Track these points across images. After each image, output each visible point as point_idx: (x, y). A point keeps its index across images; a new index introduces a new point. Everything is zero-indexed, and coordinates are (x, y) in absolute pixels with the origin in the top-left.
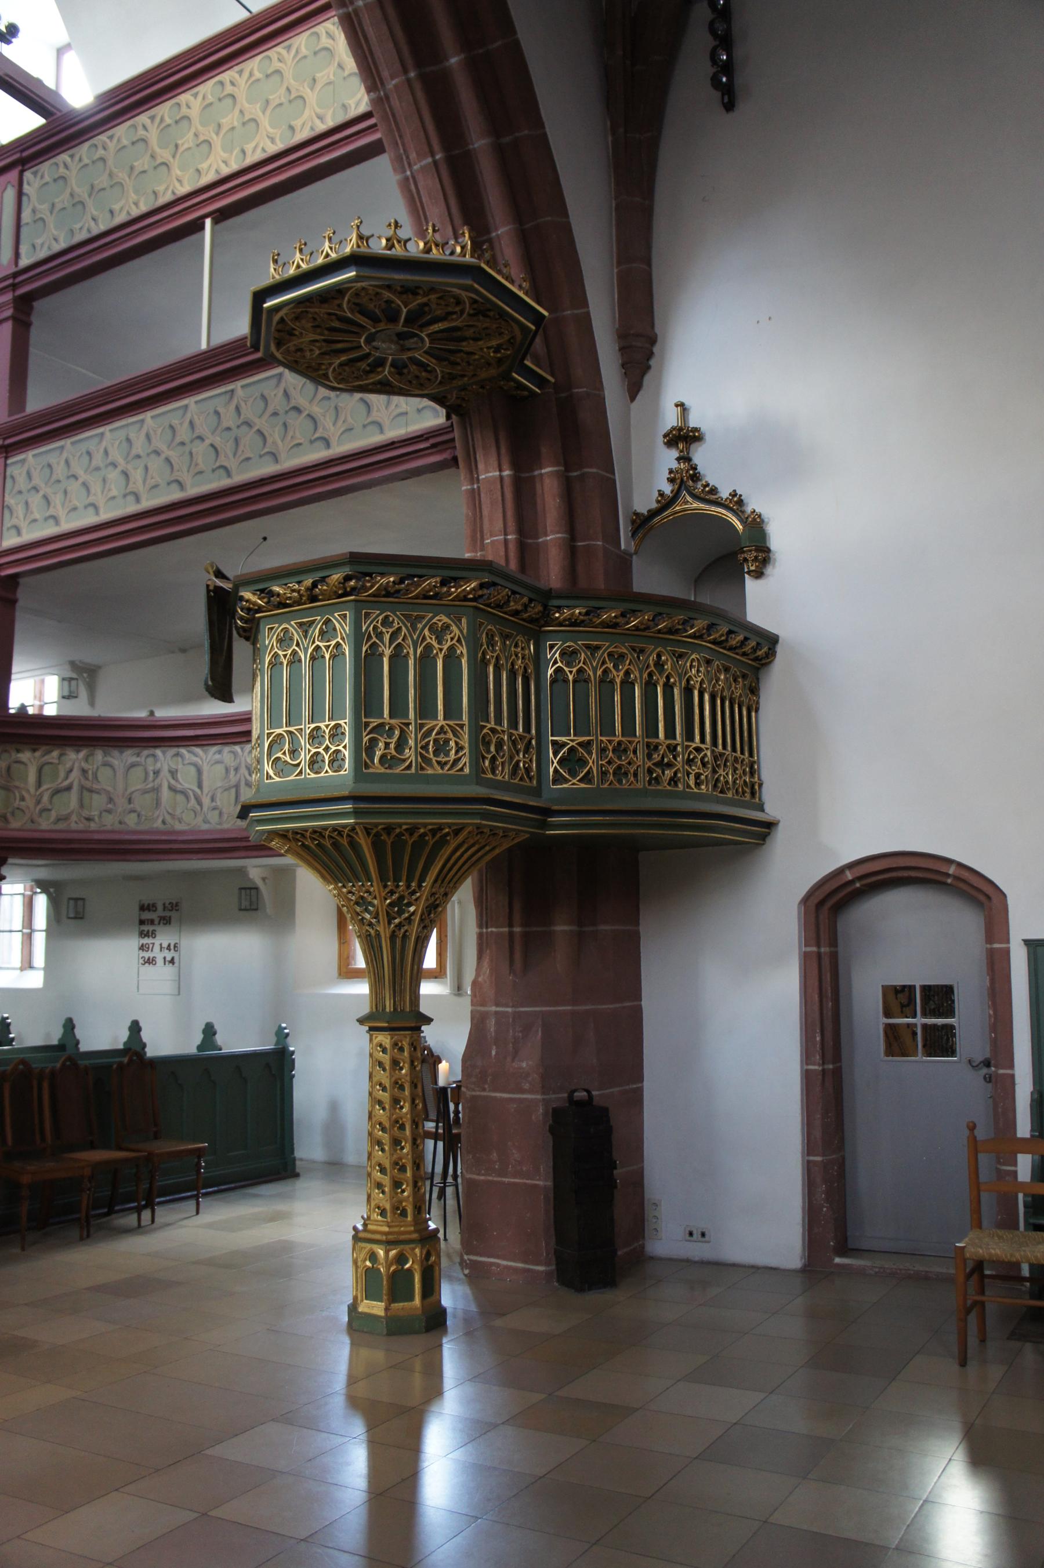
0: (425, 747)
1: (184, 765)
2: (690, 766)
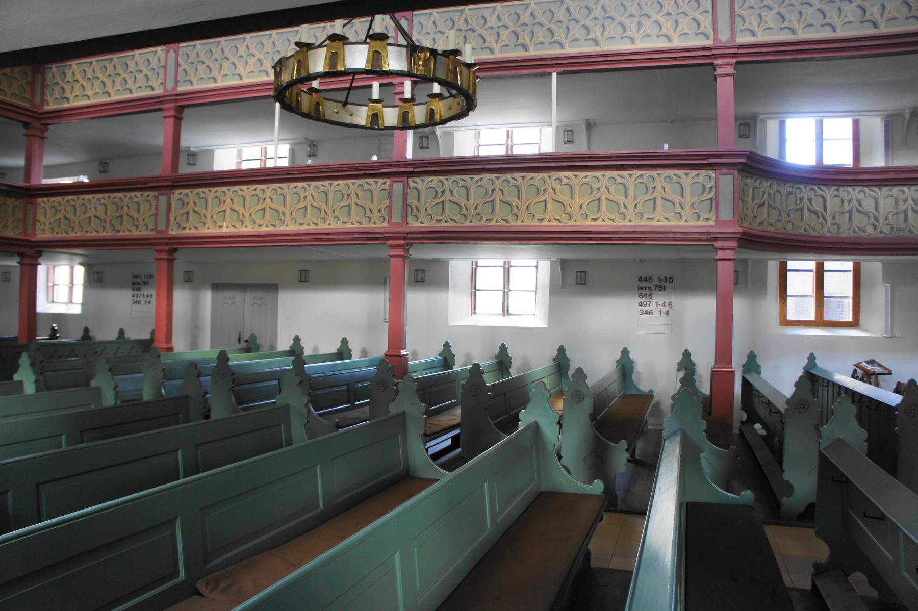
1: (816, 196)
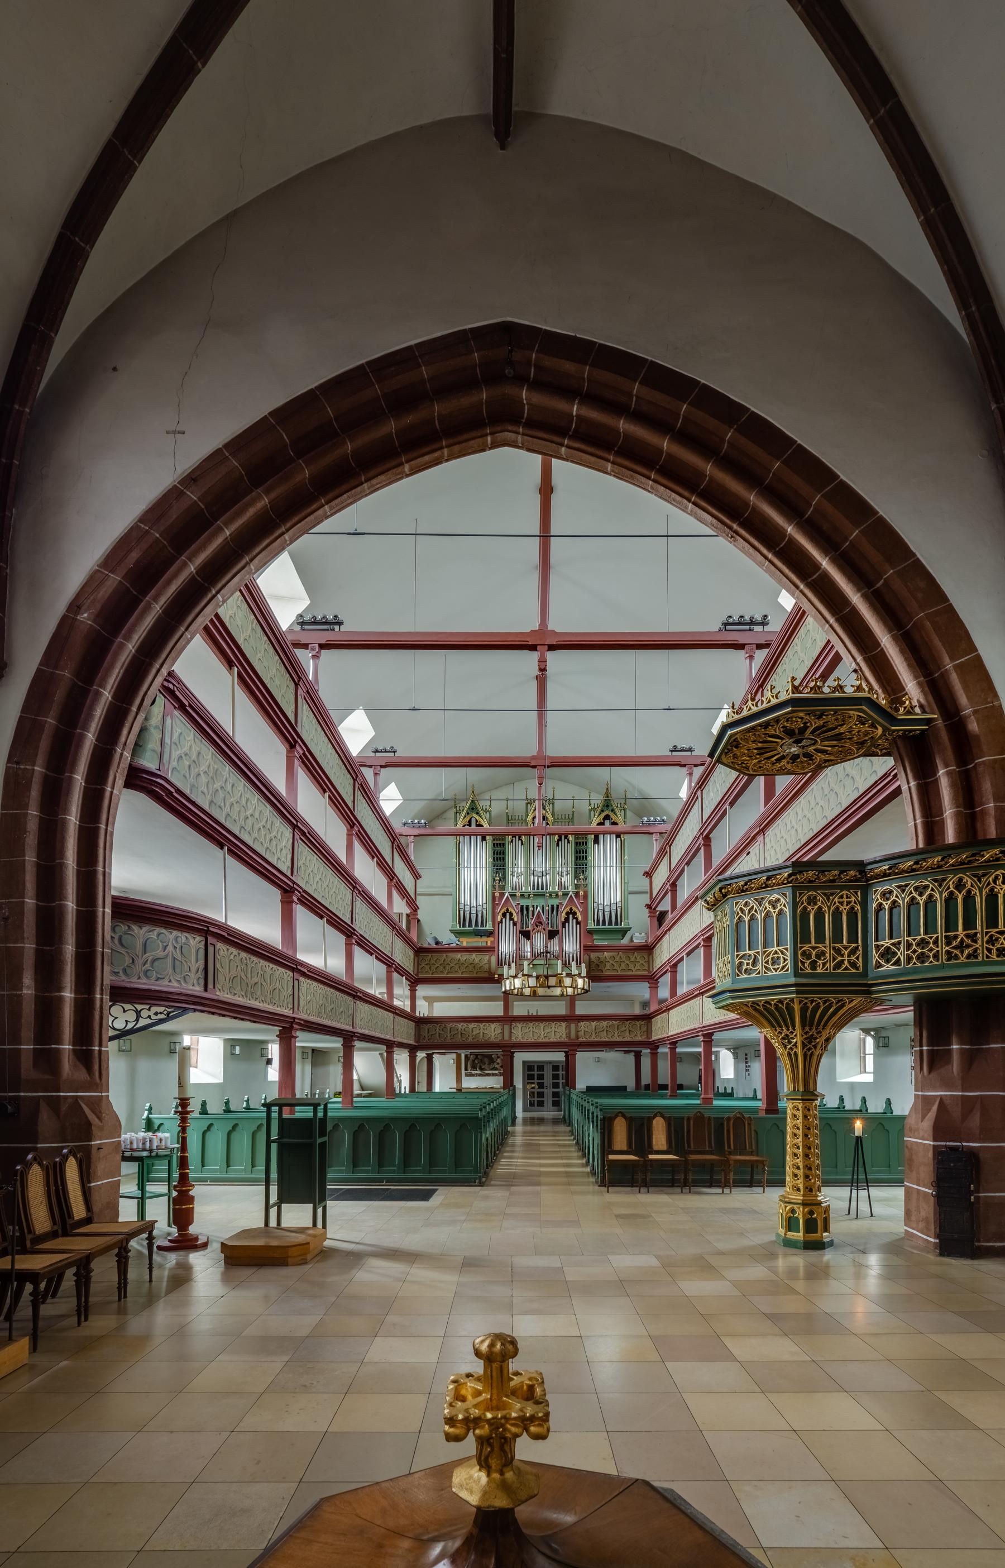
0: (767, 962)
2: (993, 945)
